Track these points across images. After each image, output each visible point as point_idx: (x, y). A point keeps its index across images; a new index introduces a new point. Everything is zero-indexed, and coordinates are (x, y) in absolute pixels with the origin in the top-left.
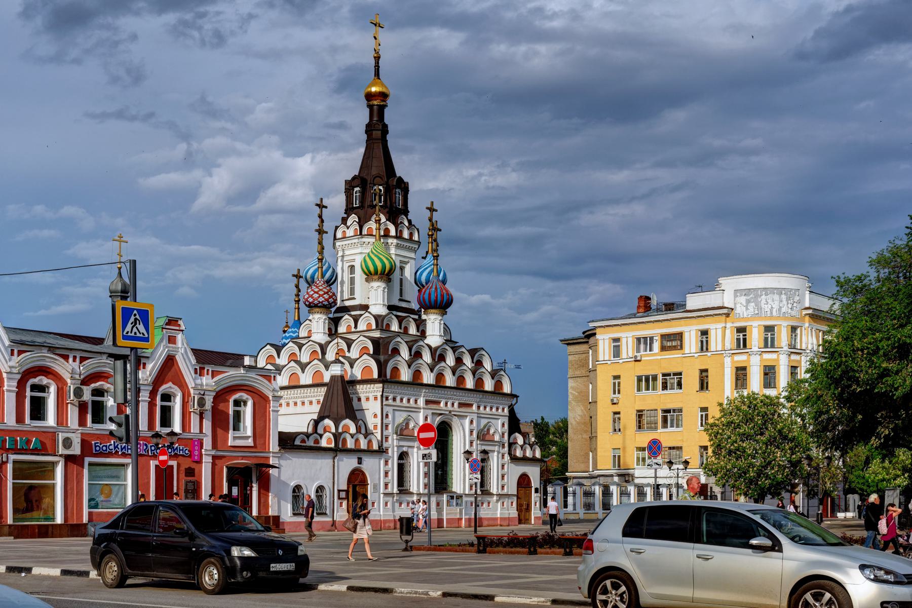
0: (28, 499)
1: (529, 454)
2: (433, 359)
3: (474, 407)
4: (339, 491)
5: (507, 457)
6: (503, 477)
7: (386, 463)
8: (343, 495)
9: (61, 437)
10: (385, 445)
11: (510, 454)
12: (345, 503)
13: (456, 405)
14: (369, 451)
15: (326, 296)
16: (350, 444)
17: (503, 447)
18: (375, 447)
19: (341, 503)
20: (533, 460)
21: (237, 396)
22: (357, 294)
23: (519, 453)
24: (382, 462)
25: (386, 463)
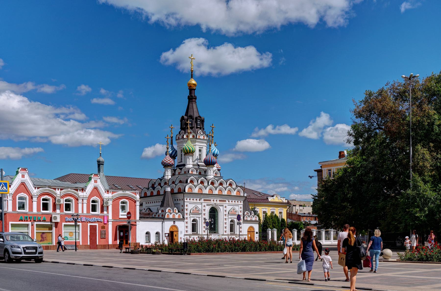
0: (42, 237)
1: (254, 219)
2: (208, 184)
3: (227, 202)
7: (187, 223)
8: (167, 235)
9: (53, 216)
10: (185, 216)
14: (179, 219)
15: (169, 162)
16: (171, 216)
18: (181, 217)
21: (123, 200)
22: (183, 161)
23: (249, 219)
25: (187, 223)
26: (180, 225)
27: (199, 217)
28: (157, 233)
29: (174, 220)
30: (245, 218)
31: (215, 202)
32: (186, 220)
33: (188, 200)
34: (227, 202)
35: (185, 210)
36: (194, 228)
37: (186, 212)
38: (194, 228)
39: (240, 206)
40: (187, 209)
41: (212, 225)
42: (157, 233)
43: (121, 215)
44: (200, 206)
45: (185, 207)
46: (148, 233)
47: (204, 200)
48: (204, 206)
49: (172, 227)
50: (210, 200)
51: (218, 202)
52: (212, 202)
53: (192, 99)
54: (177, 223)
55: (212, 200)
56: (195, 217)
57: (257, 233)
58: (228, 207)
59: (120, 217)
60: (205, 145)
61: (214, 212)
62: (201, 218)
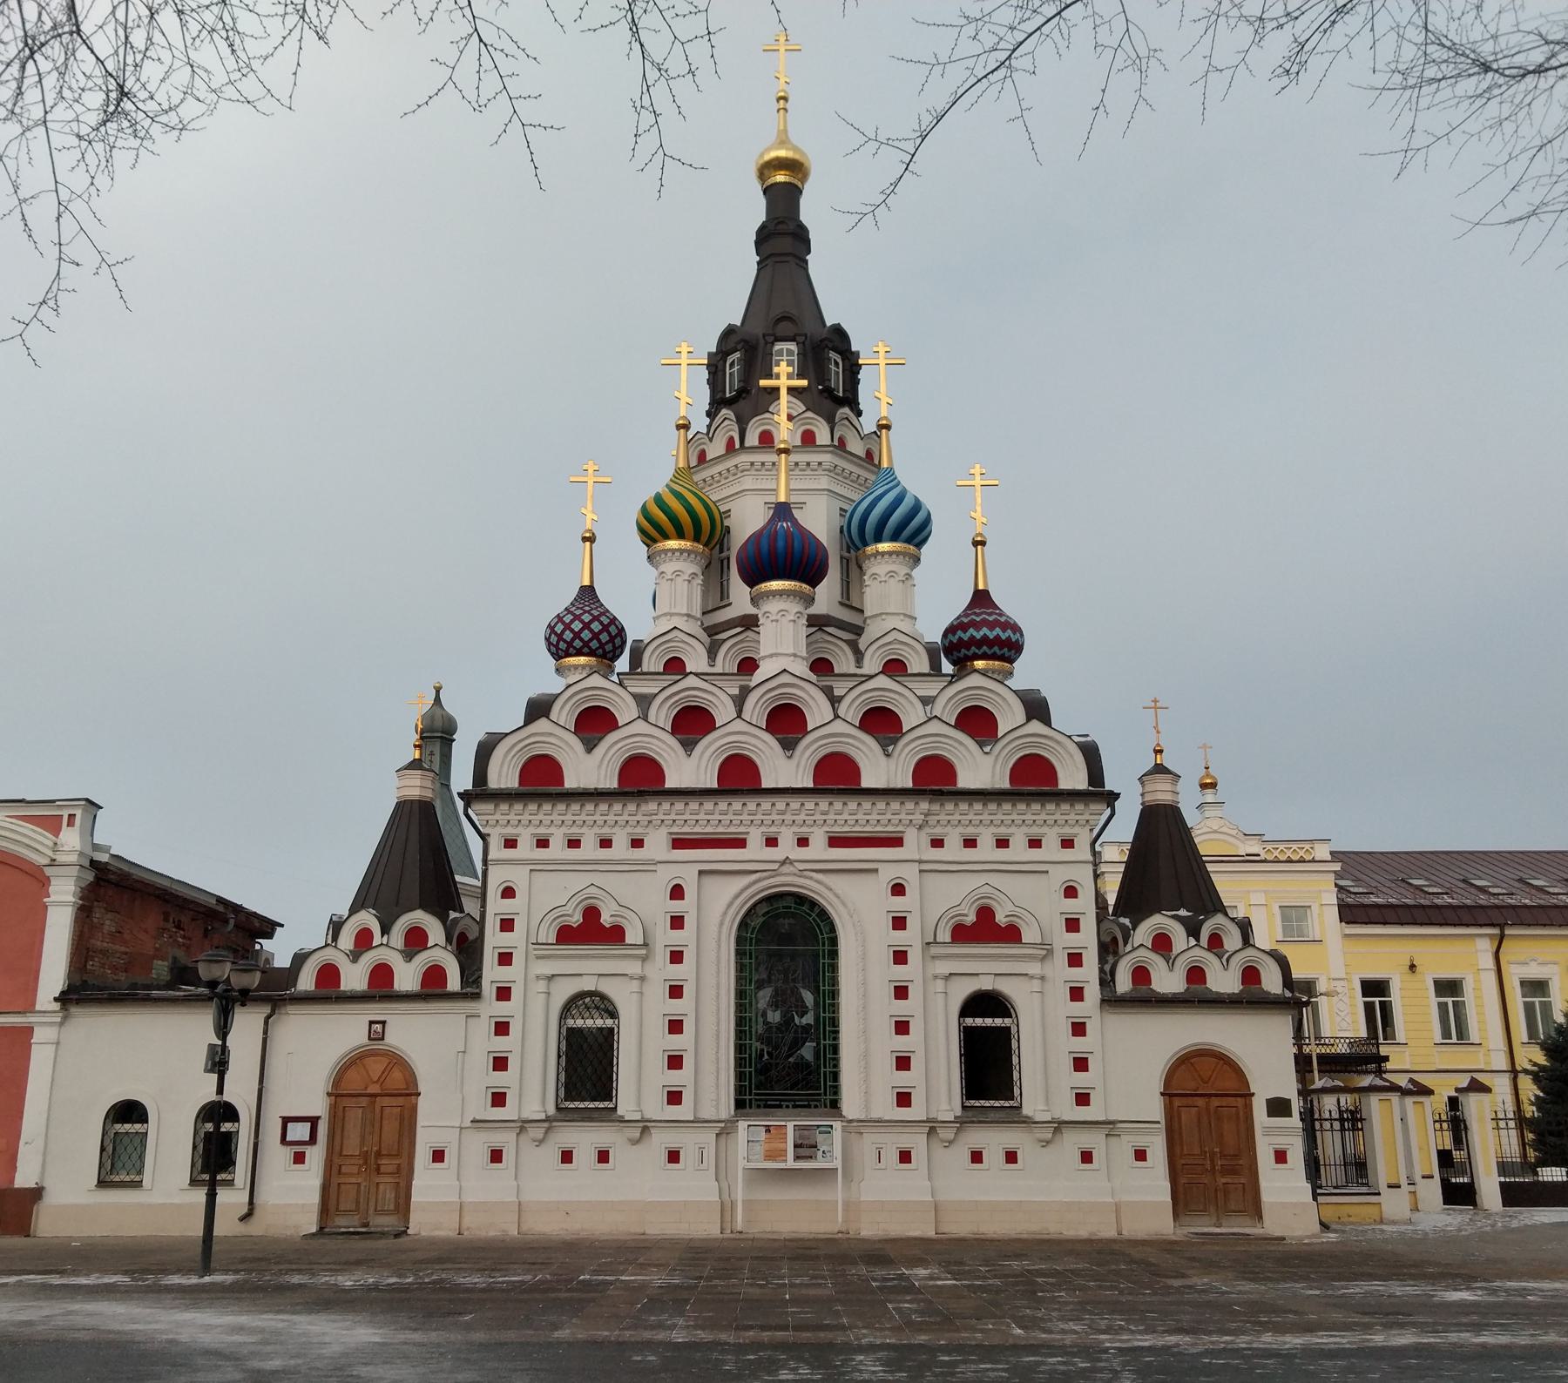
3: (915, 846)
4: (286, 1121)
5: (1093, 992)
6: (1081, 1064)
7: (502, 1028)
10: (492, 973)
11: (1107, 980)
12: (316, 1155)
13: (818, 839)
17: (1075, 960)
18: (454, 983)
19: (299, 1158)
20: (1250, 999)
24: (484, 1027)
30: (1124, 984)
31: (786, 846)
32: (491, 1008)
33: (526, 849)
35: (492, 925)
36: (587, 1067)
37: (494, 940)
38: (587, 1067)
39: (1060, 876)
40: (507, 925)
41: (797, 1044)
45: (496, 906)
46: (129, 1112)
47: (678, 843)
49: (353, 1062)
50: (740, 843)
52: (755, 849)
53: (783, 240)
54: (426, 1039)
55: (755, 839)
60: (824, 482)
61: (787, 945)
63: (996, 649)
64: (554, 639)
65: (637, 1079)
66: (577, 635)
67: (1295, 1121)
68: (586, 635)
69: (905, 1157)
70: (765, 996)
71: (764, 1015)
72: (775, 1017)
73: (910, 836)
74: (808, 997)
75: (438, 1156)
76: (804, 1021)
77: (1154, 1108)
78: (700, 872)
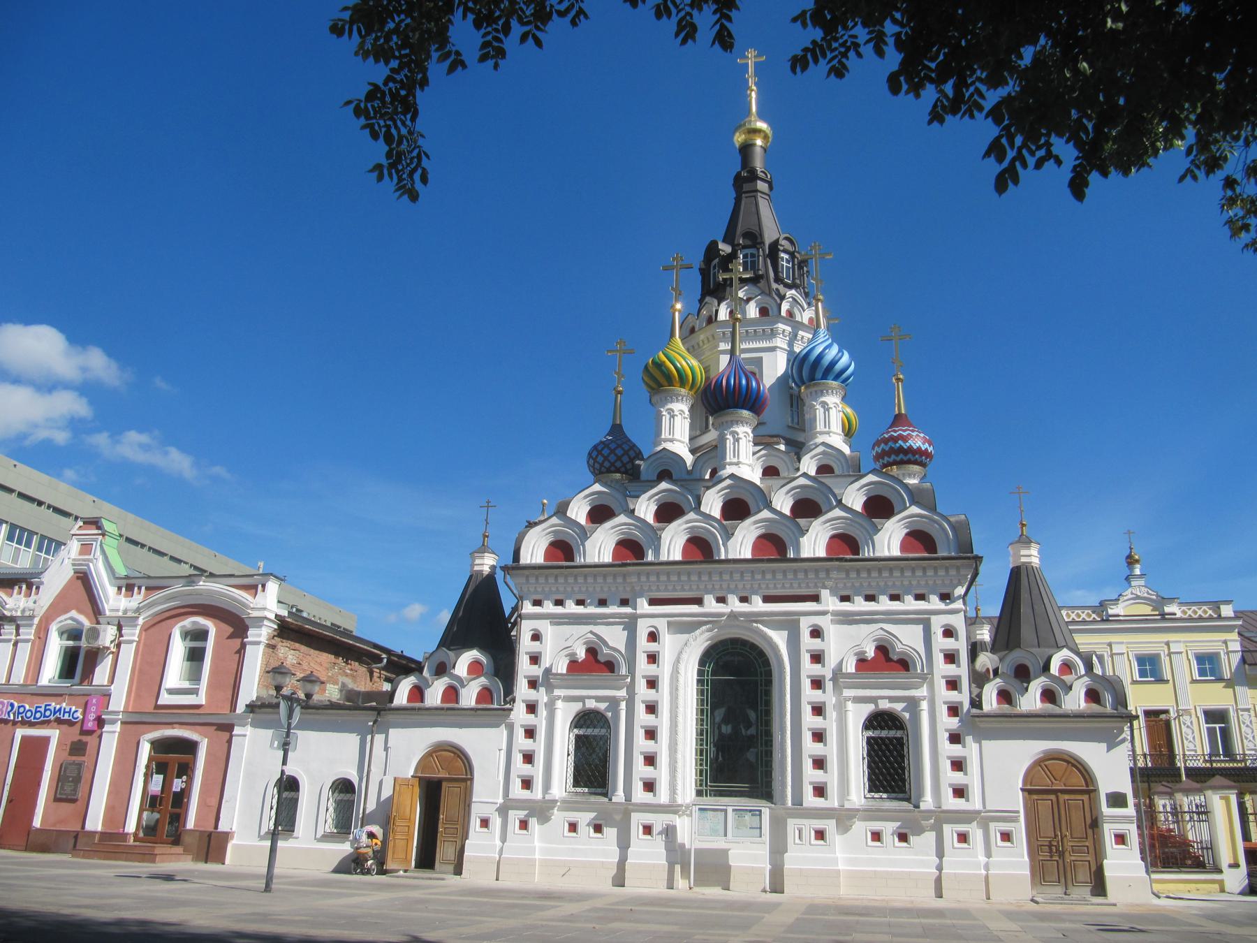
21: (188, 622)
26: (485, 746)
27: (614, 702)
28: (344, 787)
29: (450, 711)
34: (830, 602)
42: (344, 787)
43: (171, 692)
44: (615, 637)
47: (653, 602)
48: (653, 637)
51: (757, 605)
52: (711, 605)
56: (594, 697)
57: (1117, 800)
58: (833, 632)
59: (165, 699)
62: (623, 705)
63: (910, 456)
64: (591, 462)
65: (627, 772)
66: (619, 458)
67: (1130, 810)
68: (613, 458)
69: (820, 835)
70: (720, 713)
71: (719, 728)
72: (726, 729)
73: (825, 593)
74: (752, 715)
75: (485, 823)
76: (749, 732)
77: (1017, 802)
78: (669, 623)
